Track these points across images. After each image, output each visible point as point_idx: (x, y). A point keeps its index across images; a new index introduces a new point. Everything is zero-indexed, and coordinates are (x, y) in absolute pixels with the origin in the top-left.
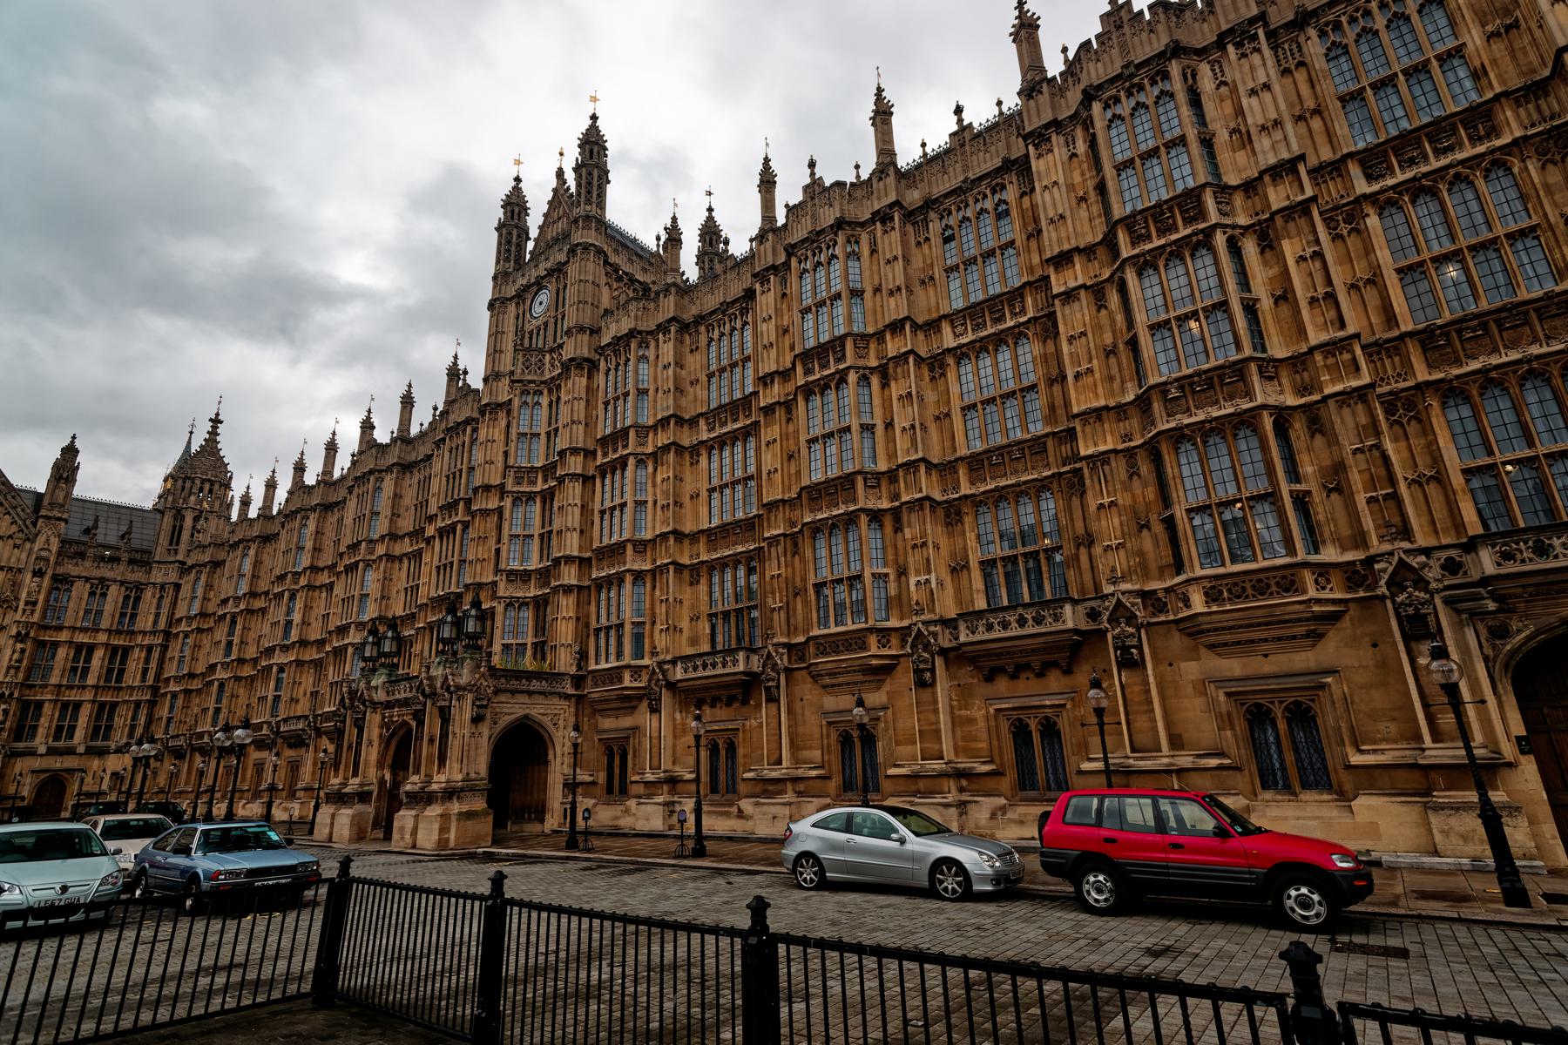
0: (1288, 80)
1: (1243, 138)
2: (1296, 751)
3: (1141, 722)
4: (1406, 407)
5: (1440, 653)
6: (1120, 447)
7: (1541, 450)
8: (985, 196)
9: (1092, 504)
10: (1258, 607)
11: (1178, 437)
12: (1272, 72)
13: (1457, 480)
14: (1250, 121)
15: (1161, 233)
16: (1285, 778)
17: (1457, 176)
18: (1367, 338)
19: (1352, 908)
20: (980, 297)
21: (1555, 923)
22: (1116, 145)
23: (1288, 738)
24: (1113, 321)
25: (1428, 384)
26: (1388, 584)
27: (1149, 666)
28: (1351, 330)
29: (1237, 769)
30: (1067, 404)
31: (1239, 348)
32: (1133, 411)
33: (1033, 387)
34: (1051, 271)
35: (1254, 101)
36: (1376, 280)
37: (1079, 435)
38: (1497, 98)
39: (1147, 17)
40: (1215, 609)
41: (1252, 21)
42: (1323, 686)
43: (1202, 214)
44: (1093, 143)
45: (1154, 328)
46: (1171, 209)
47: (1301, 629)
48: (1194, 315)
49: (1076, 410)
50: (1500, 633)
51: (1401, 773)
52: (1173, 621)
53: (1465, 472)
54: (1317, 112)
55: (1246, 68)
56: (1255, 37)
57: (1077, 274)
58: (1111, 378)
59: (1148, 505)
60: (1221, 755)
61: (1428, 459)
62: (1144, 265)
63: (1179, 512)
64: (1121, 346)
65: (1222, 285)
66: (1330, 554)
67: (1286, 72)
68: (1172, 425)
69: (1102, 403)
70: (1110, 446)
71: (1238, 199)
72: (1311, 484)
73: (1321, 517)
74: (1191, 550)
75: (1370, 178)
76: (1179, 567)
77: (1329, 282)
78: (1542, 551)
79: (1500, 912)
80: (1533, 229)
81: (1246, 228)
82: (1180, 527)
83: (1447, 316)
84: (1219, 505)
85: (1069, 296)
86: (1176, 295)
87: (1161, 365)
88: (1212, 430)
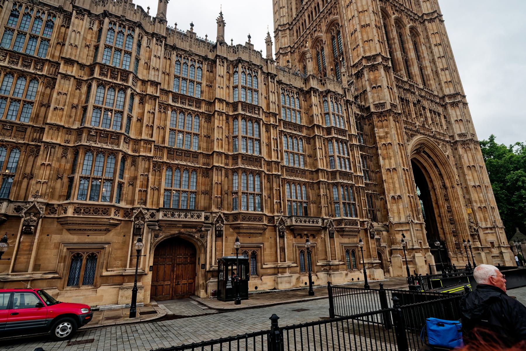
0: (165, 60)
1: (148, 67)
2: (86, 271)
3: (22, 259)
4: (158, 166)
5: (140, 240)
6: (63, 144)
7: (182, 189)
8: (44, 13)
9: (39, 162)
10: (94, 218)
11: (88, 149)
12: (162, 55)
13: (162, 191)
14: (151, 63)
15: (111, 77)
16: (78, 281)
17: (190, 113)
18: (156, 144)
19: (82, 328)
20: (21, 51)
21: (139, 321)
22: (106, 38)
23: (83, 267)
24: (80, 96)
25: (165, 162)
26: (135, 217)
27: (37, 235)
28: (153, 139)
29: (60, 278)
30: (45, 117)
31: (121, 129)
32: (74, 133)
33: (31, 103)
34: (62, 63)
35: (155, 58)
36: (164, 128)
37: (46, 132)
38: (203, 100)
39: (136, 8)
40: (76, 216)
41: (163, 37)
42: (103, 248)
43: (127, 80)
44: (100, 30)
45: (95, 107)
46: (118, 72)
47: (104, 228)
48: (111, 111)
49: (48, 121)
50: (156, 236)
51: (117, 278)
52: (58, 218)
53: (165, 190)
54: (168, 74)
55: (156, 48)
56: (161, 42)
57: (73, 71)
58: (70, 117)
59: (65, 170)
60: (56, 273)
61: (158, 183)
62: (101, 84)
63: (77, 177)
64: (80, 107)
65: (124, 106)
66: (123, 205)
67: (165, 58)
68: (88, 144)
69: (62, 124)
70: (58, 142)
71: (139, 83)
72: (125, 181)
73: (124, 192)
74: (75, 192)
75: (173, 101)
76: (68, 197)
77: (153, 123)
78: (173, 215)
79: (127, 320)
80: (198, 135)
81: (138, 93)
82: (75, 182)
83: (175, 147)
84: (93, 178)
85: (66, 77)
86: (108, 101)
87: (92, 121)
88: (101, 152)
